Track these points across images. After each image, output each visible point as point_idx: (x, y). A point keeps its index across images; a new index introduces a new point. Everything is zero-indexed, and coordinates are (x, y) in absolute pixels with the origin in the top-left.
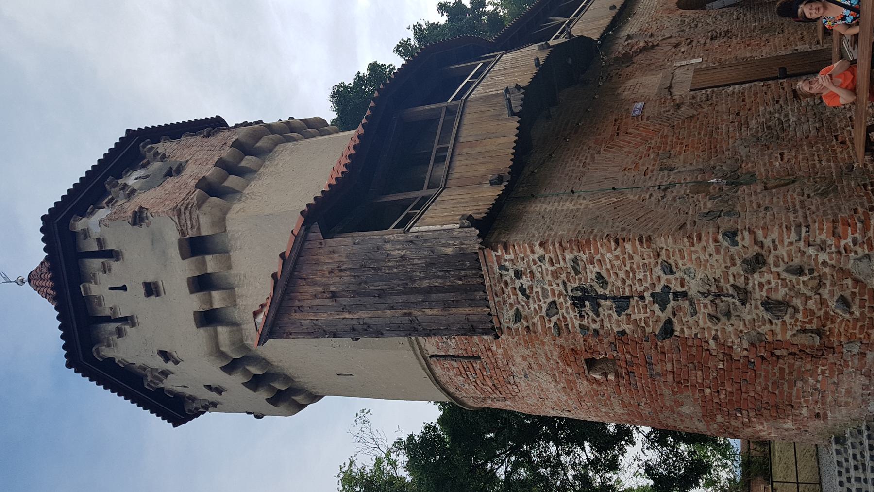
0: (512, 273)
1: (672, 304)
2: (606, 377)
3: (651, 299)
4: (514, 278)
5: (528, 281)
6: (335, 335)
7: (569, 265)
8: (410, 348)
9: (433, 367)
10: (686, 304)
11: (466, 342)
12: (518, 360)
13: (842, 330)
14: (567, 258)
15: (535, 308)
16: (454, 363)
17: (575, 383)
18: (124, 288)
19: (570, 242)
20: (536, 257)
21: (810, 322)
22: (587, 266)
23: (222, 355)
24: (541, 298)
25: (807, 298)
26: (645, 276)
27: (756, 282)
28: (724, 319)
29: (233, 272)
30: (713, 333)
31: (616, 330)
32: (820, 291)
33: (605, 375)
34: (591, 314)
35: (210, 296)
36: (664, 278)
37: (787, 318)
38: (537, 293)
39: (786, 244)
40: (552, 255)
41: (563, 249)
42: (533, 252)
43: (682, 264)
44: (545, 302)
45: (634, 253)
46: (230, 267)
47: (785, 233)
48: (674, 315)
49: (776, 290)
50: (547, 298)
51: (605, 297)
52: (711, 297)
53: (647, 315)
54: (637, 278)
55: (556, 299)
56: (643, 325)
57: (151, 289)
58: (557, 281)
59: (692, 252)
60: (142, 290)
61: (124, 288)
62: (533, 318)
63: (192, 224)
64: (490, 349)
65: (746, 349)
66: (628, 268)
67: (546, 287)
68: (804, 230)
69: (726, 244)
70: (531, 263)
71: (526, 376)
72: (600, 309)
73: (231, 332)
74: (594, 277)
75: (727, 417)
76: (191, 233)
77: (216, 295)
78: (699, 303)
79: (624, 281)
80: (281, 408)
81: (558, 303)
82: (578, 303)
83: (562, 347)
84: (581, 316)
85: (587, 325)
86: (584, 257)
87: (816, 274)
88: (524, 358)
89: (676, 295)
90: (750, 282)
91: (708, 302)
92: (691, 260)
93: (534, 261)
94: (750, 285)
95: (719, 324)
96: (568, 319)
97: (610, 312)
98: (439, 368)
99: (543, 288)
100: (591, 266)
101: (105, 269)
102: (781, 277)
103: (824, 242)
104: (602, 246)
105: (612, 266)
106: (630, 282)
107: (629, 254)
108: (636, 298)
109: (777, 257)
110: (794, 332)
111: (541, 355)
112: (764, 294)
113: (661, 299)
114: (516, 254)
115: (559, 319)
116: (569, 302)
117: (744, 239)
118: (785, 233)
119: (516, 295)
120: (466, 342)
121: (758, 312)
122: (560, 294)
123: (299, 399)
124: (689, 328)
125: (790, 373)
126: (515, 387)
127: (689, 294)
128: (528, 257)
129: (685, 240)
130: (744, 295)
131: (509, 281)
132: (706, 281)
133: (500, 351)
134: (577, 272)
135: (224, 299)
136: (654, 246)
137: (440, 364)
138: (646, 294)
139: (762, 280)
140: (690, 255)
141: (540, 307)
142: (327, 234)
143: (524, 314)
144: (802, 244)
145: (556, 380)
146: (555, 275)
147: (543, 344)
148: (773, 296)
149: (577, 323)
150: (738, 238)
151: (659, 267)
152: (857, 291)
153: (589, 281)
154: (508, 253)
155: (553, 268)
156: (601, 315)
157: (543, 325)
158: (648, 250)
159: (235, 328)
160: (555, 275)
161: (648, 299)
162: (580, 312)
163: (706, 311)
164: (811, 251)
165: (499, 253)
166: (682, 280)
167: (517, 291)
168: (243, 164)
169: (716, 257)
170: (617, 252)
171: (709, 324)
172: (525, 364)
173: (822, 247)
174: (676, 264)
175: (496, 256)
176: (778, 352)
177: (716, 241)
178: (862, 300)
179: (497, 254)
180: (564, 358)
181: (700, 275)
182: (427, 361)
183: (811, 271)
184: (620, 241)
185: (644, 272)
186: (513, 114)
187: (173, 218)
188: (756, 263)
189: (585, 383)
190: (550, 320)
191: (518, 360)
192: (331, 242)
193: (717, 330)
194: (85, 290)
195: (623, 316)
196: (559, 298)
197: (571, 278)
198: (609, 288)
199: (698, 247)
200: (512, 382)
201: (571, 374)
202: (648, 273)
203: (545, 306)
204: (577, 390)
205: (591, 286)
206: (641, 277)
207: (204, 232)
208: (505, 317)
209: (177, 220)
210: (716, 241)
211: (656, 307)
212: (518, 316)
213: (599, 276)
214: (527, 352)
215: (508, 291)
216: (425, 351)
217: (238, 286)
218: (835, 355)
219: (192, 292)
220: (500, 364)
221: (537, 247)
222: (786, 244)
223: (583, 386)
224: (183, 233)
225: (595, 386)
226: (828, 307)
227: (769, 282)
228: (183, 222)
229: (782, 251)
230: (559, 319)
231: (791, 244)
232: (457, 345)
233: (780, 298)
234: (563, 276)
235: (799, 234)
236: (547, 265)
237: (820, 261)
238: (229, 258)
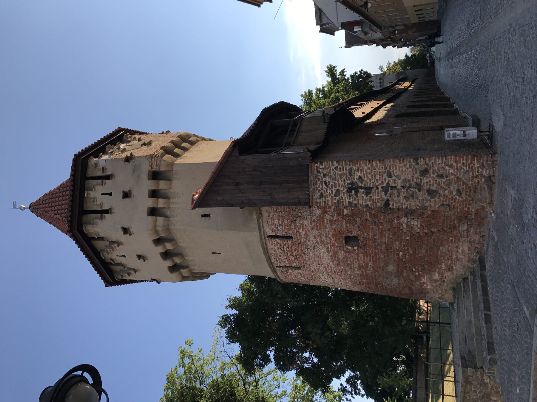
0: (322, 175)
1: (390, 191)
2: (354, 248)
3: (381, 189)
4: (323, 177)
5: (329, 179)
6: (232, 206)
7: (347, 172)
8: (258, 231)
9: (268, 243)
10: (395, 192)
11: (288, 228)
12: (312, 238)
13: (458, 205)
14: (347, 168)
15: (330, 193)
16: (279, 241)
17: (337, 253)
18: (110, 194)
19: (350, 161)
20: (334, 167)
21: (446, 201)
22: (356, 172)
23: (156, 232)
24: (333, 187)
25: (445, 189)
26: (380, 178)
27: (425, 182)
28: (411, 199)
29: (171, 191)
30: (406, 206)
31: (364, 204)
32: (450, 186)
33: (353, 247)
34: (354, 196)
35: (158, 200)
36: (388, 179)
37: (436, 198)
38: (332, 185)
39: (437, 164)
40: (341, 167)
41: (346, 164)
42: (333, 165)
43: (396, 173)
44: (335, 190)
45: (376, 167)
46: (170, 188)
47: (437, 159)
48: (390, 196)
49: (433, 185)
50: (336, 188)
51: (361, 188)
52: (406, 189)
53: (379, 197)
54: (376, 179)
55: (340, 188)
56: (377, 202)
57: (126, 195)
58: (341, 179)
59: (400, 167)
60: (121, 195)
61: (110, 194)
62: (328, 197)
63: (157, 164)
64: (298, 232)
65: (419, 228)
66: (373, 174)
67: (336, 182)
68: (444, 158)
69: (414, 164)
70: (331, 170)
71: (314, 249)
72: (359, 194)
73: (164, 220)
74: (358, 178)
75: (408, 272)
76: (155, 169)
77: (161, 200)
78: (401, 191)
79: (370, 180)
80: (175, 275)
81: (340, 190)
82: (349, 190)
83: (335, 230)
84: (350, 197)
85: (352, 202)
86: (355, 168)
87: (448, 178)
88: (315, 237)
89: (392, 187)
90: (423, 181)
91: (405, 191)
92: (399, 170)
93: (333, 169)
94: (423, 183)
95: (409, 202)
96: (344, 199)
97: (363, 195)
98: (270, 243)
99: (334, 183)
100: (357, 172)
102: (435, 180)
103: (452, 165)
104: (363, 163)
105: (366, 172)
106: (373, 181)
107: (374, 167)
108: (375, 189)
109: (434, 170)
110: (439, 205)
111: (323, 235)
112: (428, 187)
113: (386, 189)
114: (325, 166)
115: (340, 198)
116: (345, 190)
117: (421, 162)
118: (437, 159)
119: (322, 185)
120: (288, 228)
121: (425, 196)
122: (342, 186)
123: (184, 272)
124: (396, 203)
125: (438, 242)
126: (307, 257)
127: (397, 187)
128: (330, 168)
129: (398, 161)
130: (419, 186)
131: (320, 178)
132: (405, 181)
133: (304, 232)
134: (351, 175)
135: (164, 203)
136: (385, 163)
137: (272, 241)
138: (379, 187)
139: (427, 181)
140: (399, 168)
141: (332, 191)
142: (241, 154)
143: (324, 195)
144: (443, 164)
145: (328, 251)
147: (326, 228)
148: (432, 188)
149: (347, 200)
150: (419, 161)
151: (385, 175)
152: (464, 187)
153: (356, 179)
154: (322, 165)
155: (340, 173)
156: (359, 197)
157: (332, 201)
158: (382, 165)
159: (167, 219)
160: (341, 176)
161: (380, 189)
162: (350, 195)
163: (404, 195)
164: (447, 168)
165: (318, 165)
166: (395, 180)
167: (323, 183)
168: (182, 145)
169: (410, 170)
170: (369, 166)
171: (405, 201)
172: (314, 241)
173: (451, 166)
174: (393, 173)
175: (316, 166)
176: (433, 230)
177: (410, 162)
178: (466, 191)
179: (317, 165)
180: (334, 236)
181: (402, 178)
182: (265, 238)
183: (447, 177)
184: (371, 161)
185: (380, 176)
186: (324, 122)
187: (149, 159)
188: (425, 172)
189: (343, 252)
190: (335, 198)
191: (312, 238)
192: (242, 157)
193: (408, 205)
194: (87, 194)
195: (368, 197)
196: (341, 188)
197: (348, 178)
198: (364, 183)
199: (402, 165)
200: (306, 253)
201: (337, 246)
202: (381, 177)
203: (334, 191)
204: (338, 257)
205: (356, 182)
206: (378, 178)
207: (162, 169)
208: (316, 196)
209: (150, 161)
210: (410, 162)
211: (383, 193)
212: (321, 196)
213: (360, 177)
214: (317, 233)
215: (319, 183)
216: (266, 233)
217: (173, 198)
218: (457, 231)
219: (149, 197)
220: (302, 241)
221: (335, 163)
222: (437, 164)
223: (341, 254)
225: (347, 254)
226: (453, 194)
227: (430, 181)
228: (153, 162)
229: (436, 168)
230: (340, 198)
231: (439, 164)
232: (283, 230)
233: (434, 189)
234: (344, 177)
235: (442, 160)
236: (338, 171)
237: (450, 172)
238: (171, 184)
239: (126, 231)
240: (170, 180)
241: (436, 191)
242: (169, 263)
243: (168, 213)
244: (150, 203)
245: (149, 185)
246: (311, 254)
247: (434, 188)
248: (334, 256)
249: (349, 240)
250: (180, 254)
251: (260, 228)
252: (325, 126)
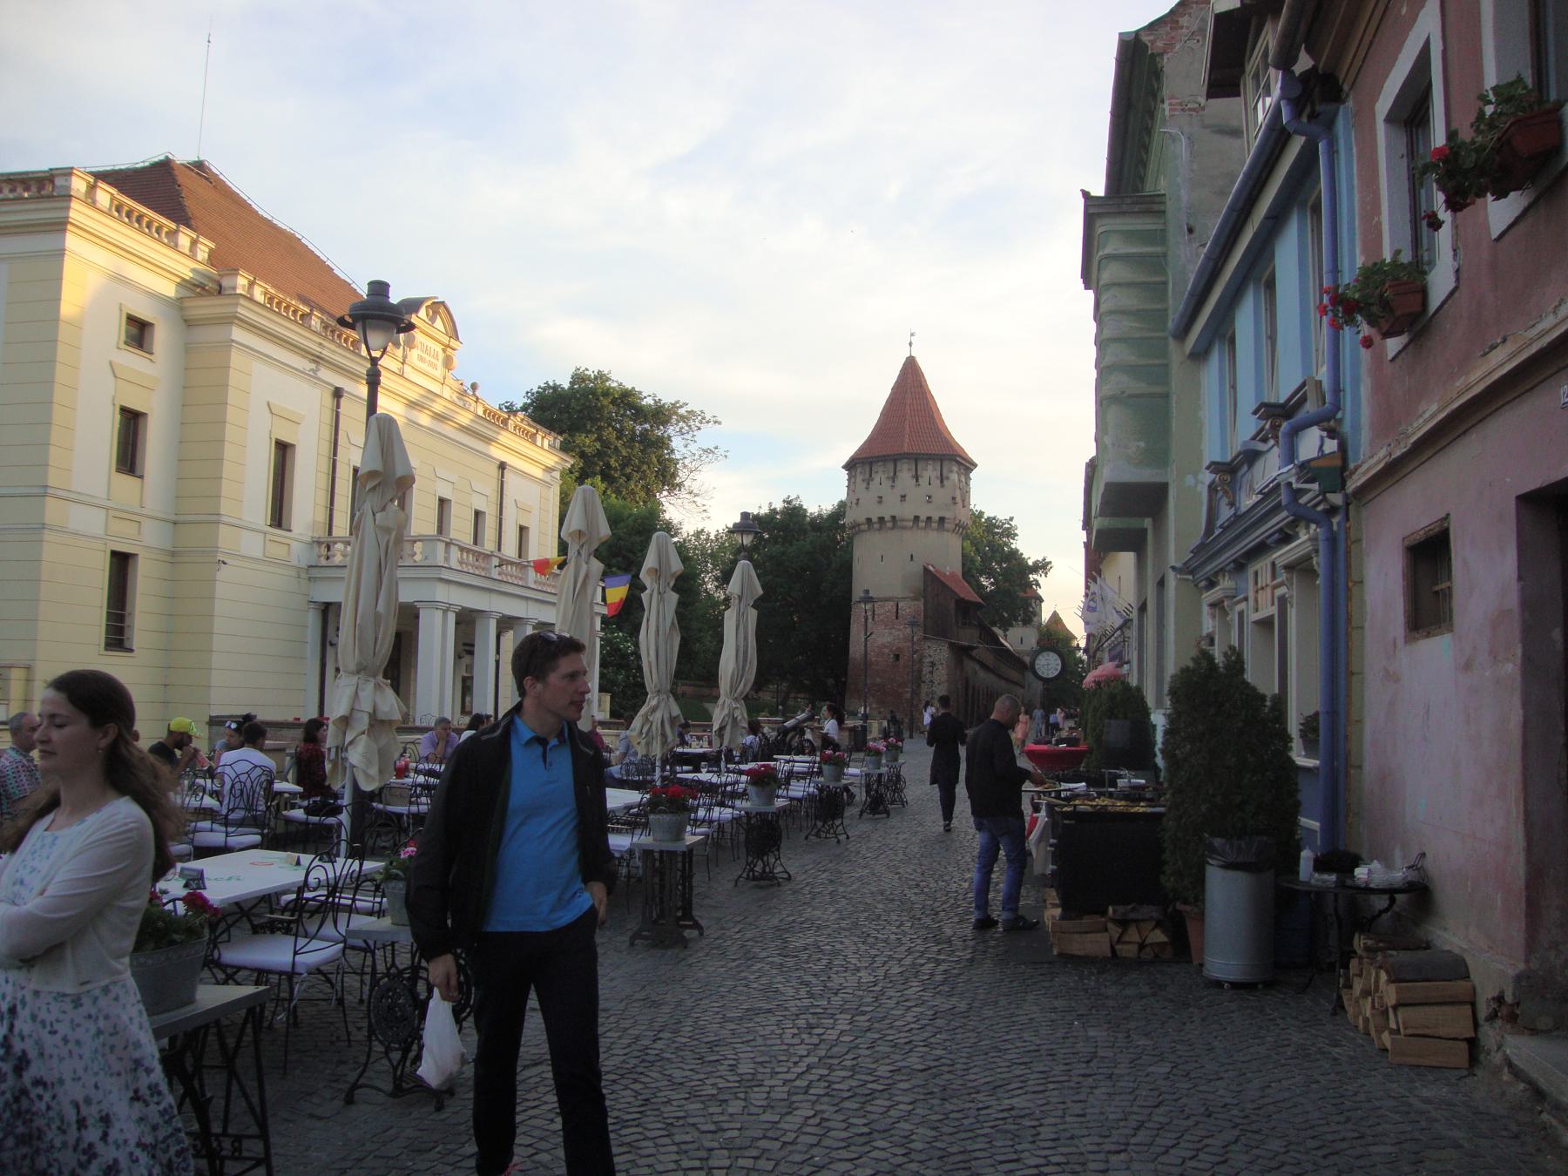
82: (932, 662)
101: (937, 478)
180: (898, 648)
207: (946, 525)
239: (903, 497)
242: (875, 519)
243: (915, 528)
244: (923, 518)
245: (936, 517)
248: (884, 646)
249: (897, 657)
251: (904, 599)
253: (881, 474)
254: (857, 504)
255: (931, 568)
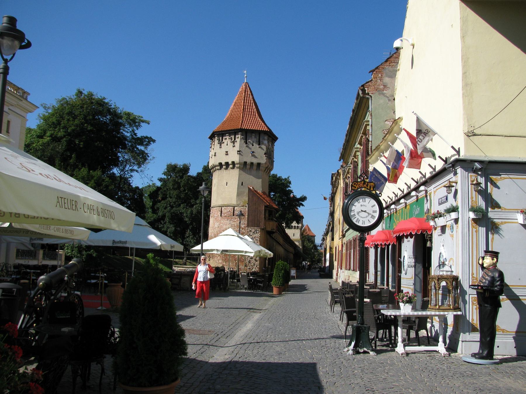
16: (232, 211)
76: (261, 165)
77: (249, 167)
146: (256, 237)
186: (271, 229)
191: (234, 223)
212: (250, 231)
224: (262, 164)
240: (256, 169)
241: (250, 263)
246: (228, 222)
247: (251, 262)
250: (227, 168)
251: (238, 206)
252: (270, 230)
253: (227, 140)
254: (215, 155)
255: (251, 188)
